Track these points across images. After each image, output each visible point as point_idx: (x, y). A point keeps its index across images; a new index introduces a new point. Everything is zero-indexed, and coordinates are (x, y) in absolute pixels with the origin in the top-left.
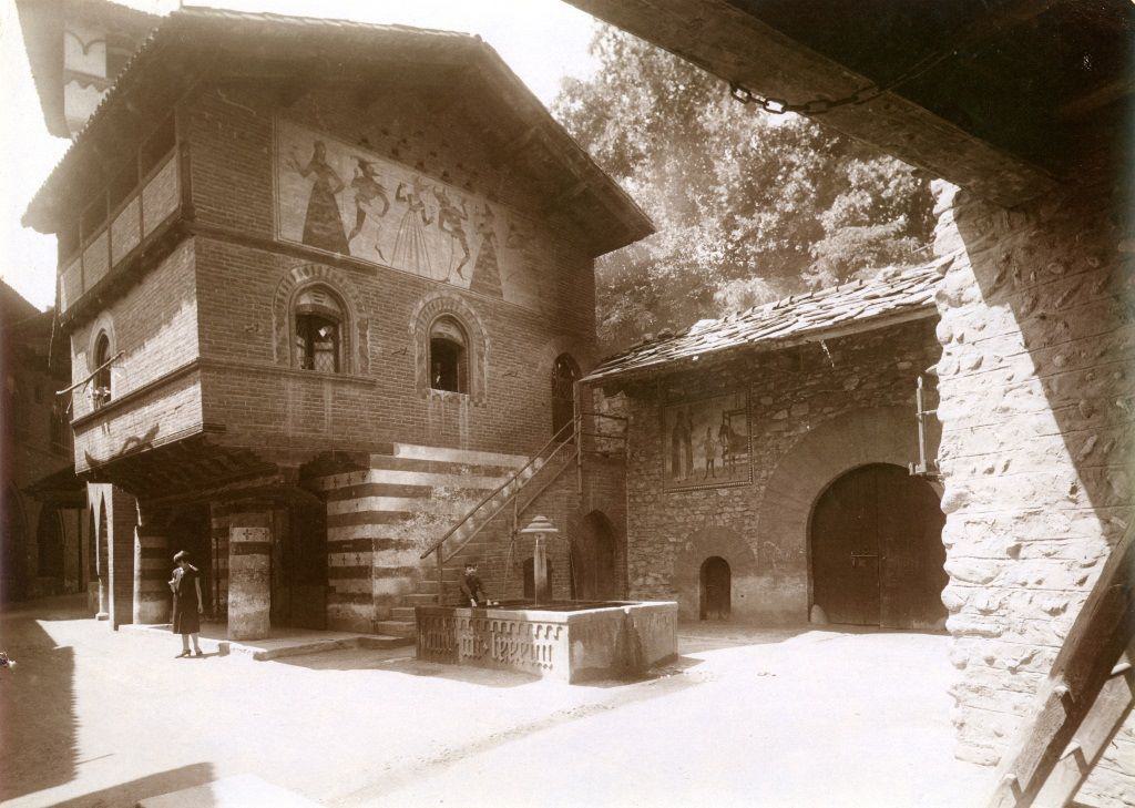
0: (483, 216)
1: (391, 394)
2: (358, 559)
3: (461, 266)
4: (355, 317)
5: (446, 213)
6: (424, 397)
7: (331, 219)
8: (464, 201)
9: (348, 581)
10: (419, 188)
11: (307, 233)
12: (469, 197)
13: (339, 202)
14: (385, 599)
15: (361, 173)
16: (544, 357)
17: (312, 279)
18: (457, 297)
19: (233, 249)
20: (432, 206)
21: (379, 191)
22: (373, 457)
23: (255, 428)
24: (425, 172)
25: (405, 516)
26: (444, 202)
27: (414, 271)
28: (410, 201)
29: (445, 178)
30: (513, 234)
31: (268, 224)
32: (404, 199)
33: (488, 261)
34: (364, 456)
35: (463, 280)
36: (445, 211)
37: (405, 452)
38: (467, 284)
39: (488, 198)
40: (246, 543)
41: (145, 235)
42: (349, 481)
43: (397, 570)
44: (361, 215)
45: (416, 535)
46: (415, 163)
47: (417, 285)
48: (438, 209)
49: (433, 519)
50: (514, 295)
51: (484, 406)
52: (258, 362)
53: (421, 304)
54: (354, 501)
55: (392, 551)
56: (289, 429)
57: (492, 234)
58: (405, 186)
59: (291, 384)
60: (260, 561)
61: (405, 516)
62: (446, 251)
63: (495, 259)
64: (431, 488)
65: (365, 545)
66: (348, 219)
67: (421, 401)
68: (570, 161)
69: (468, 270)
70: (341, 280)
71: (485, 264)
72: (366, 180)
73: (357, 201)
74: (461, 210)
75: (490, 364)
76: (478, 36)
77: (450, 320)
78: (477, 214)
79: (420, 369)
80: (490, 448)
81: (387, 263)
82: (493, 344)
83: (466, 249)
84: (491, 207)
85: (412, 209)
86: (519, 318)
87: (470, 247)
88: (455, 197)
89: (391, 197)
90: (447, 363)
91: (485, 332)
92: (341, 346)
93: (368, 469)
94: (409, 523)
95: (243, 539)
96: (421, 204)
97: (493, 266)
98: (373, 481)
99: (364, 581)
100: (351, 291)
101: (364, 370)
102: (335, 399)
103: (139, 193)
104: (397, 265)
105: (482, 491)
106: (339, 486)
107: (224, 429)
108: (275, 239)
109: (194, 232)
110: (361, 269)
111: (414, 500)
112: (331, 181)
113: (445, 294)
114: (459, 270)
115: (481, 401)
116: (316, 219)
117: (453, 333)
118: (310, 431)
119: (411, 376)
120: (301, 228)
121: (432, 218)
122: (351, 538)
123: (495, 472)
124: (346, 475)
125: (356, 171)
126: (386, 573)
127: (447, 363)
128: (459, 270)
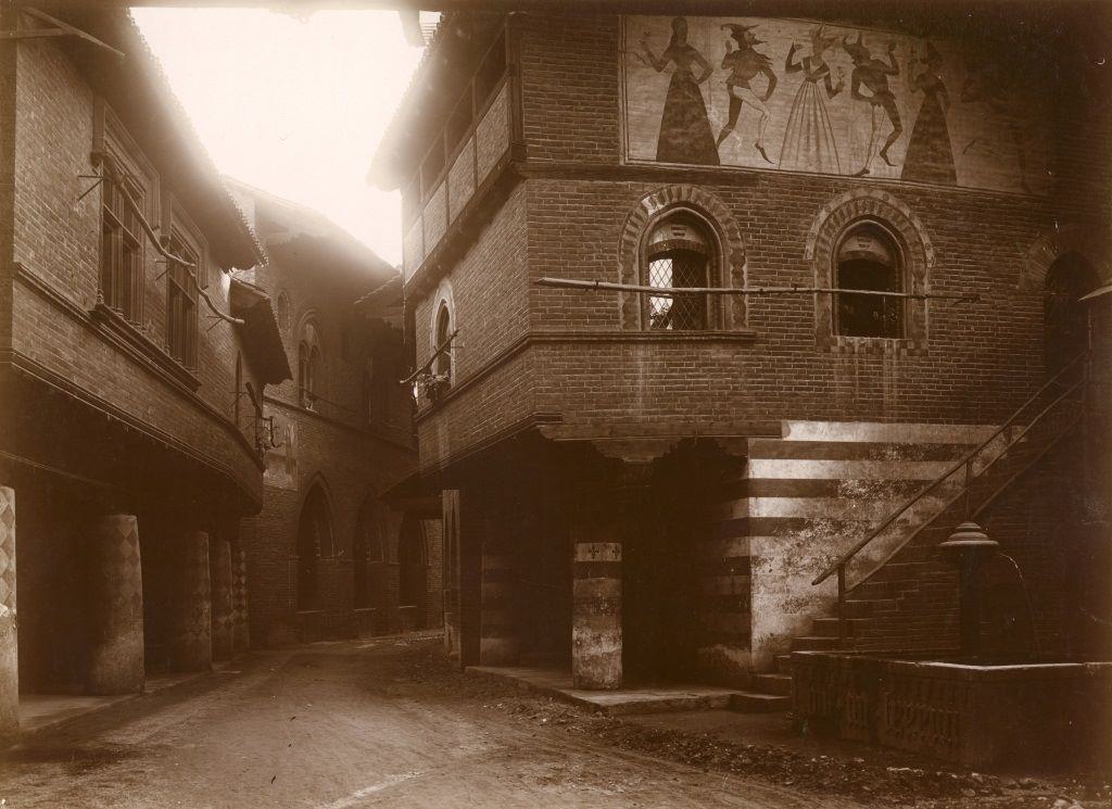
1: (776, 350)
6: (827, 350)
7: (694, 119)
8: (892, 46)
11: (664, 145)
13: (705, 94)
31: (612, 144)
32: (798, 67)
34: (740, 443)
37: (799, 432)
38: (897, 171)
44: (735, 104)
48: (850, 69)
53: (823, 215)
56: (637, 410)
58: (800, 47)
59: (641, 353)
66: (717, 115)
69: (899, 151)
81: (773, 164)
82: (937, 255)
85: (812, 79)
87: (901, 113)
89: (778, 68)
96: (824, 68)
97: (935, 135)
100: (721, 211)
108: (622, 163)
109: (526, 174)
111: (812, 501)
112: (695, 67)
114: (883, 154)
118: (665, 413)
120: (655, 141)
121: (842, 84)
125: (728, 45)
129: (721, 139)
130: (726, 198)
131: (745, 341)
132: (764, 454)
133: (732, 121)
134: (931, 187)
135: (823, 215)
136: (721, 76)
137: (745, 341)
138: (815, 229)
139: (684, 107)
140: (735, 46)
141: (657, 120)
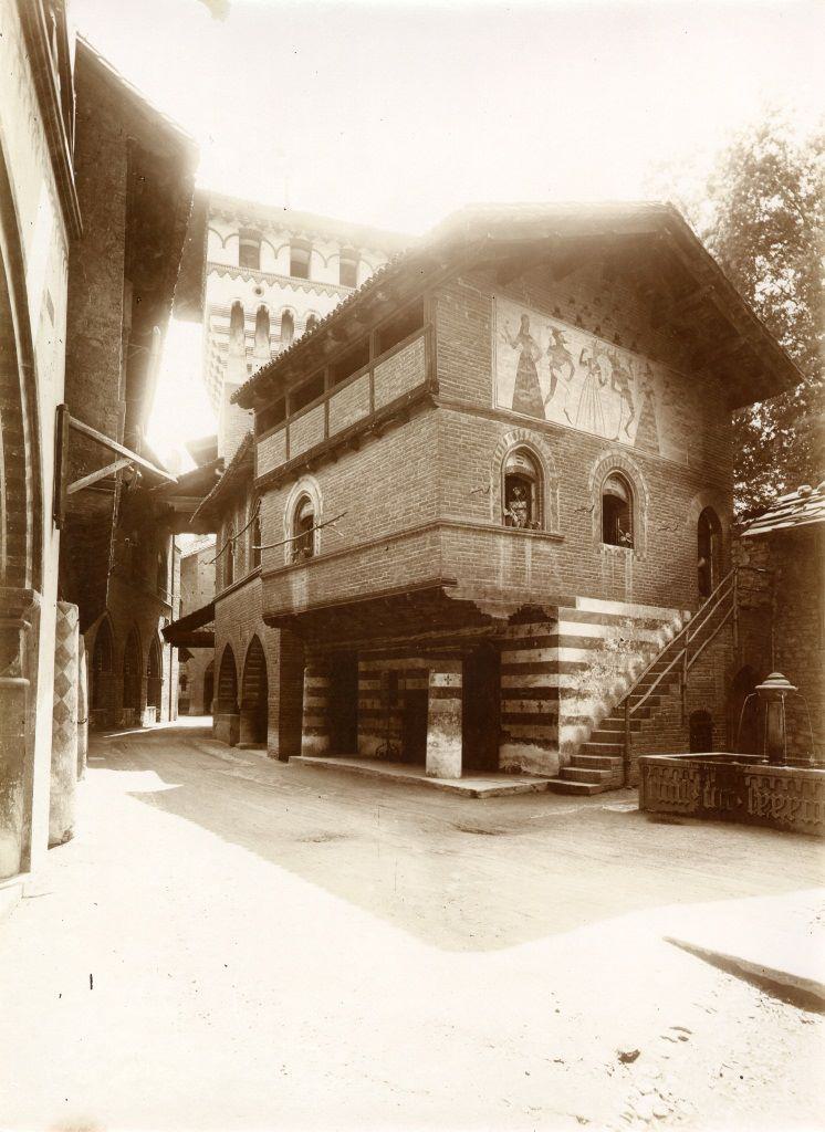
0: (645, 375)
1: (573, 549)
2: (540, 706)
3: (628, 424)
4: (550, 476)
5: (618, 374)
6: (599, 552)
7: (533, 386)
8: (631, 361)
9: (526, 728)
10: (597, 352)
11: (516, 399)
12: (634, 357)
13: (538, 370)
14: (569, 745)
15: (554, 340)
16: (693, 509)
17: (518, 443)
18: (624, 455)
19: (465, 418)
20: (606, 367)
21: (567, 357)
22: (561, 609)
23: (477, 582)
24: (602, 336)
25: (584, 667)
26: (615, 364)
27: (592, 432)
28: (590, 365)
29: (617, 341)
30: (668, 390)
31: (488, 393)
33: (649, 419)
34: (553, 609)
35: (628, 440)
36: (615, 372)
37: (585, 604)
38: (631, 442)
39: (649, 358)
40: (447, 688)
41: (376, 409)
42: (530, 632)
43: (577, 718)
44: (554, 380)
45: (593, 686)
46: (594, 329)
47: (595, 444)
48: (610, 371)
49: (604, 670)
50: (667, 451)
51: (644, 561)
52: (481, 521)
53: (597, 462)
54: (537, 652)
55: (573, 700)
56: (500, 582)
57: (652, 392)
60: (455, 704)
61: (584, 667)
62: (617, 411)
63: (653, 416)
64: (603, 640)
65: (553, 694)
66: (544, 384)
67: (596, 556)
68: (733, 317)
69: (633, 428)
70: (539, 443)
71: (647, 420)
72: (558, 347)
73: (551, 368)
74: (628, 370)
75: (649, 519)
76: (669, 203)
77: (618, 477)
78: (640, 373)
79: (596, 525)
80: (647, 602)
83: (632, 408)
84: (651, 365)
86: (668, 471)
88: (623, 356)
89: (575, 361)
90: (616, 517)
91: (645, 488)
92: (533, 504)
93: (556, 621)
94: (587, 674)
95: (444, 684)
96: (598, 367)
97: (650, 422)
98: (561, 633)
99: (547, 727)
100: (546, 452)
101: (555, 527)
102: (534, 554)
103: (371, 371)
104: (581, 427)
105: (642, 643)
106: (516, 637)
107: (455, 583)
110: (553, 432)
111: (590, 651)
112: (533, 351)
113: (616, 452)
114: (626, 429)
115: (642, 555)
116: (522, 387)
117: (618, 490)
118: (515, 585)
119: (589, 532)
121: (606, 379)
122: (532, 686)
123: (653, 625)
124: (527, 626)
126: (570, 721)
127: (616, 517)
128: (626, 429)
129: (546, 402)
130: (549, 443)
131: (558, 540)
132: (566, 618)
133: (552, 393)
134: (648, 454)
135: (597, 462)
136: (546, 360)
137: (558, 540)
138: (593, 471)
139: (526, 379)
140: (554, 342)
141: (512, 381)
